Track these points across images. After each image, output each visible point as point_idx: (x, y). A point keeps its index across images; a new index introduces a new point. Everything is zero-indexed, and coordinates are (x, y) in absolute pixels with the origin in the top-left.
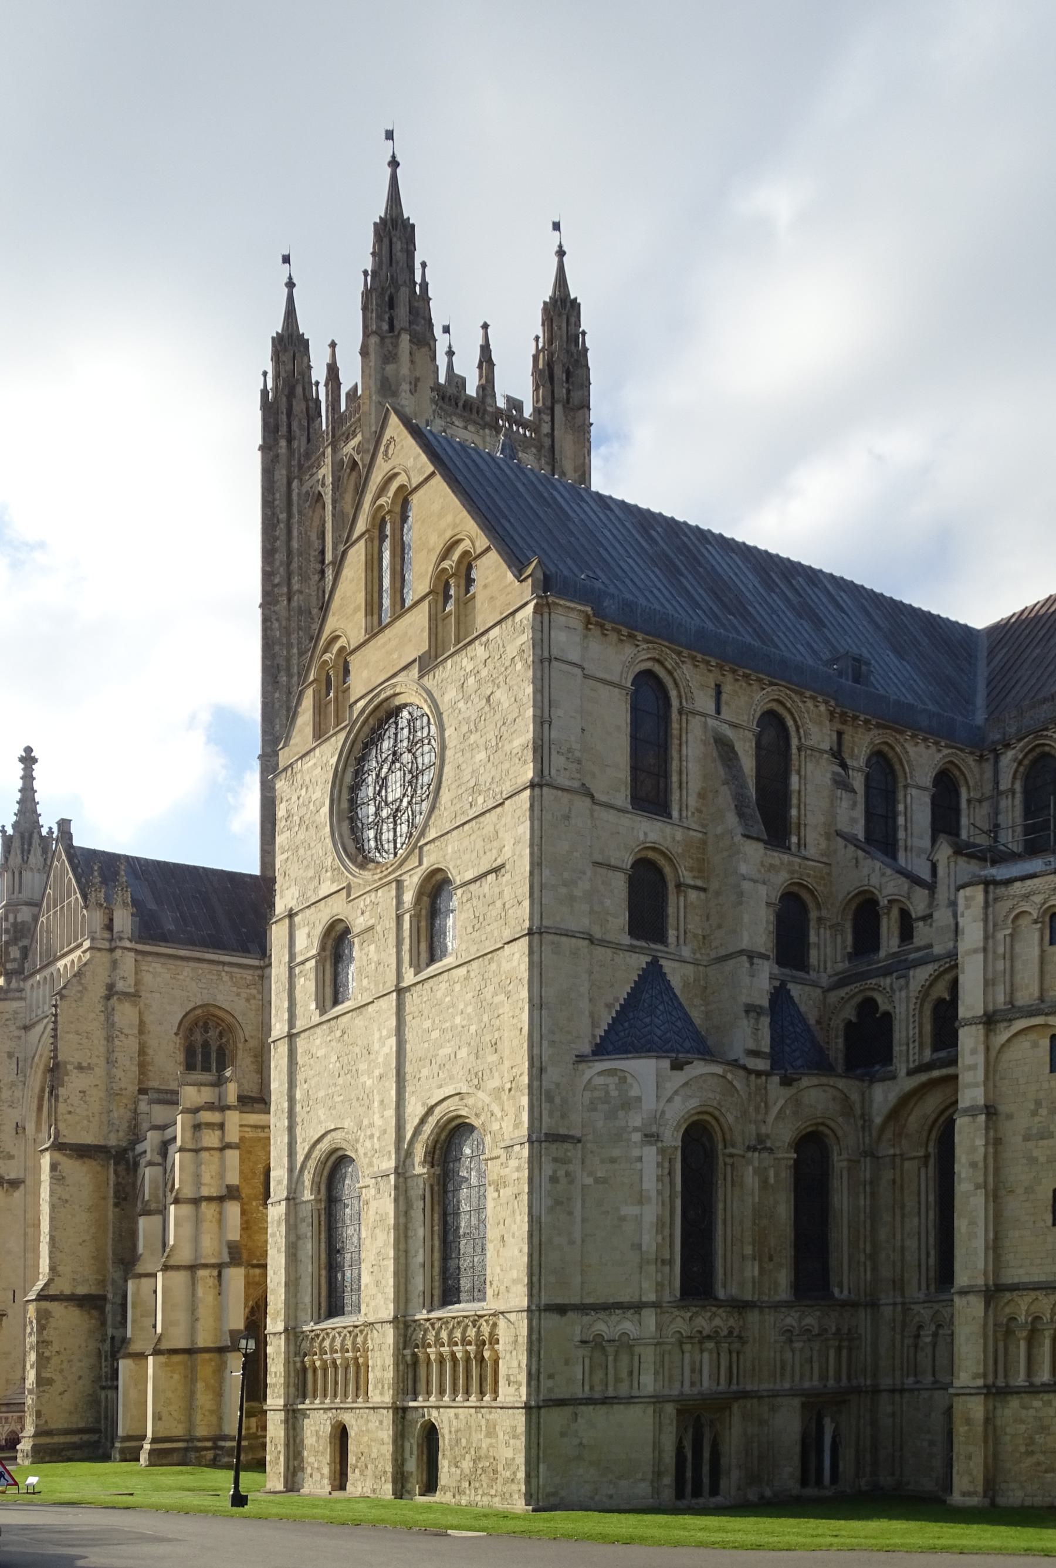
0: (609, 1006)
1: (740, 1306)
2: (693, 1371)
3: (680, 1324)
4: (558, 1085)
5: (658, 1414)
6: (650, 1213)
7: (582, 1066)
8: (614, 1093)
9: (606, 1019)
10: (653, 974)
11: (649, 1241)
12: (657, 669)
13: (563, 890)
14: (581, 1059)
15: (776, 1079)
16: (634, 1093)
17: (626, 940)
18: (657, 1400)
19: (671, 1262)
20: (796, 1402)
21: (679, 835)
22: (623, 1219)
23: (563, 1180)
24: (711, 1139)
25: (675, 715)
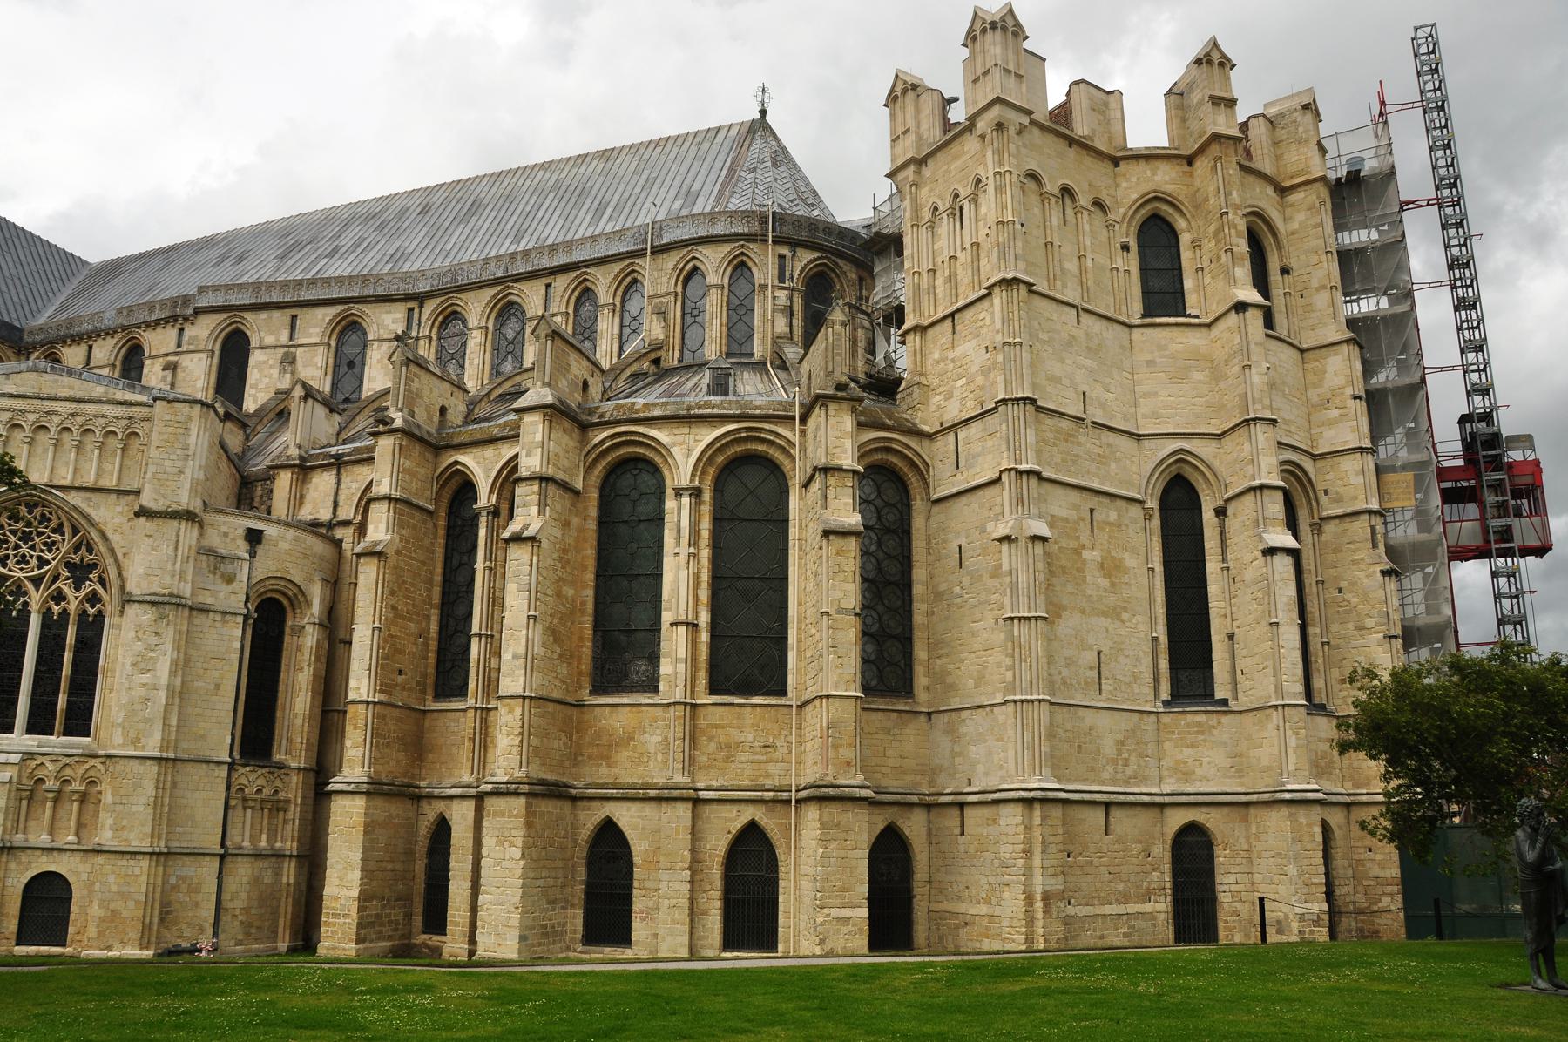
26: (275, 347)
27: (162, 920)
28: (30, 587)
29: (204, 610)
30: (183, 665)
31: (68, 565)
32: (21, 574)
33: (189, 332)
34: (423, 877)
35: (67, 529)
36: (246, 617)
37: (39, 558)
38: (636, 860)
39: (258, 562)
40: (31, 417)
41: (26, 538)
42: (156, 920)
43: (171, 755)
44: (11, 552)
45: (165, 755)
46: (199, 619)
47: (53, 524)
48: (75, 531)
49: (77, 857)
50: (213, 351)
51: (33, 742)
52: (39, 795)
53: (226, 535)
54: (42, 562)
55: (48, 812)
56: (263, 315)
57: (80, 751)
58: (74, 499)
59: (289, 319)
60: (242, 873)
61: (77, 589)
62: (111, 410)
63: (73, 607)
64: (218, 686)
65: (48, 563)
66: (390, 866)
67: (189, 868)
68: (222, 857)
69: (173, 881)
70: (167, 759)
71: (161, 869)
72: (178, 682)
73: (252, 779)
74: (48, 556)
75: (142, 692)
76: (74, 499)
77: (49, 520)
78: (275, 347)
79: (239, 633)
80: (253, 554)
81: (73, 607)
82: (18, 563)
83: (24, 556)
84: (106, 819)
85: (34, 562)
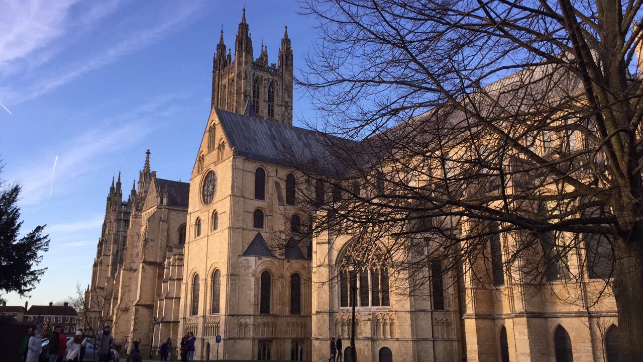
0: (247, 244)
1: (275, 316)
2: (262, 332)
3: (260, 320)
4: (233, 262)
5: (254, 342)
6: (252, 293)
7: (239, 258)
8: (246, 265)
9: (246, 247)
10: (259, 236)
11: (252, 300)
12: (262, 167)
13: (236, 218)
14: (239, 256)
15: (286, 261)
16: (250, 264)
17: (252, 228)
18: (254, 339)
19: (258, 305)
20: (290, 341)
21: (266, 204)
22: (247, 294)
23: (234, 285)
24: (270, 275)
25: (266, 177)
34: (500, 346)
38: (572, 339)
51: (374, 308)
60: (440, 346)
63: (379, 267)
66: (487, 343)
68: (433, 341)
70: (413, 311)
73: (439, 315)
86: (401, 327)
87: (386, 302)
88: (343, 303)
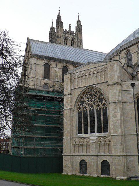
26: (136, 52)
27: (127, 170)
28: (93, 104)
29: (125, 102)
30: (123, 114)
31: (99, 99)
32: (91, 103)
33: (120, 55)
35: (98, 92)
36: (135, 102)
37: (94, 99)
39: (135, 90)
40: (88, 73)
41: (91, 95)
42: (126, 170)
43: (124, 134)
44: (89, 99)
45: (122, 134)
46: (125, 104)
47: (95, 92)
48: (99, 92)
49: (109, 157)
50: (125, 57)
52: (101, 145)
53: (127, 86)
54: (95, 99)
55: (103, 148)
56: (132, 47)
57: (107, 135)
58: (97, 86)
59: (137, 46)
61: (101, 103)
62: (100, 68)
63: (101, 107)
64: (131, 118)
65: (95, 99)
67: (132, 159)
69: (129, 162)
70: (123, 135)
71: (125, 159)
72: (122, 118)
74: (95, 98)
75: (115, 121)
76: (97, 86)
77: (94, 91)
78: (136, 52)
79: (134, 106)
80: (133, 89)
81: (101, 107)
82: (91, 100)
83: (91, 99)
84: (113, 149)
85: (93, 100)
86: (115, 146)
87: (106, 130)
88: (80, 132)
